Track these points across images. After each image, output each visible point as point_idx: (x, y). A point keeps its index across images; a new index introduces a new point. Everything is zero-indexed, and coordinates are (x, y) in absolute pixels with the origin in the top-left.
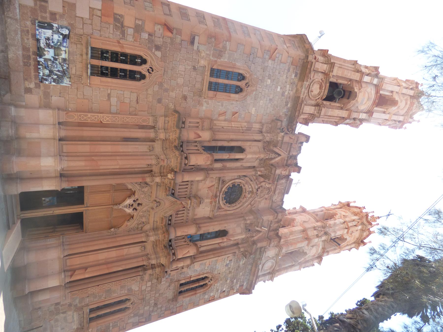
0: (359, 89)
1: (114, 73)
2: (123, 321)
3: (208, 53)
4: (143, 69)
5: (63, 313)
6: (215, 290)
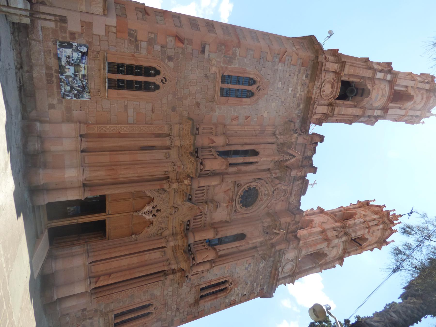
0: (373, 86)
1: (130, 86)
3: (218, 60)
4: (156, 80)
5: (90, 318)
6: (236, 293)
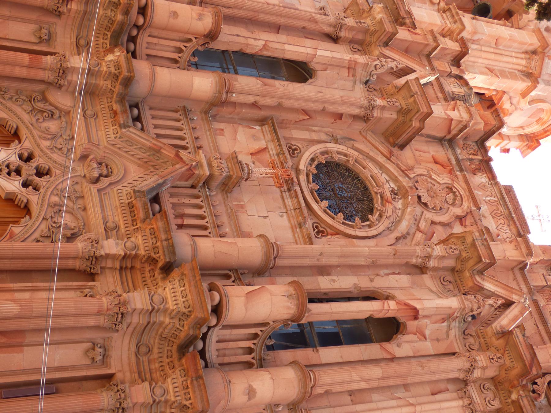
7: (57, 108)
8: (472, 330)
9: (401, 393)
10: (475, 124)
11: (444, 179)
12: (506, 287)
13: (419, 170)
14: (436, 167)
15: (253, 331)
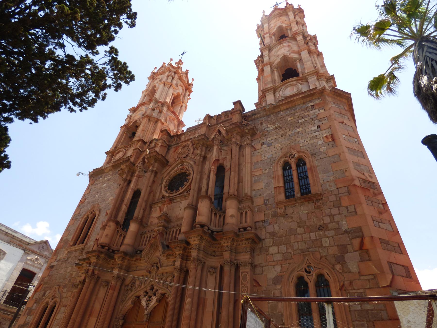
2: (351, 283)
4: (51, 304)
6: (312, 142)
7: (132, 281)
8: (226, 143)
9: (242, 166)
10: (164, 138)
11: (180, 149)
12: (214, 131)
13: (176, 157)
14: (176, 151)
15: (213, 214)
